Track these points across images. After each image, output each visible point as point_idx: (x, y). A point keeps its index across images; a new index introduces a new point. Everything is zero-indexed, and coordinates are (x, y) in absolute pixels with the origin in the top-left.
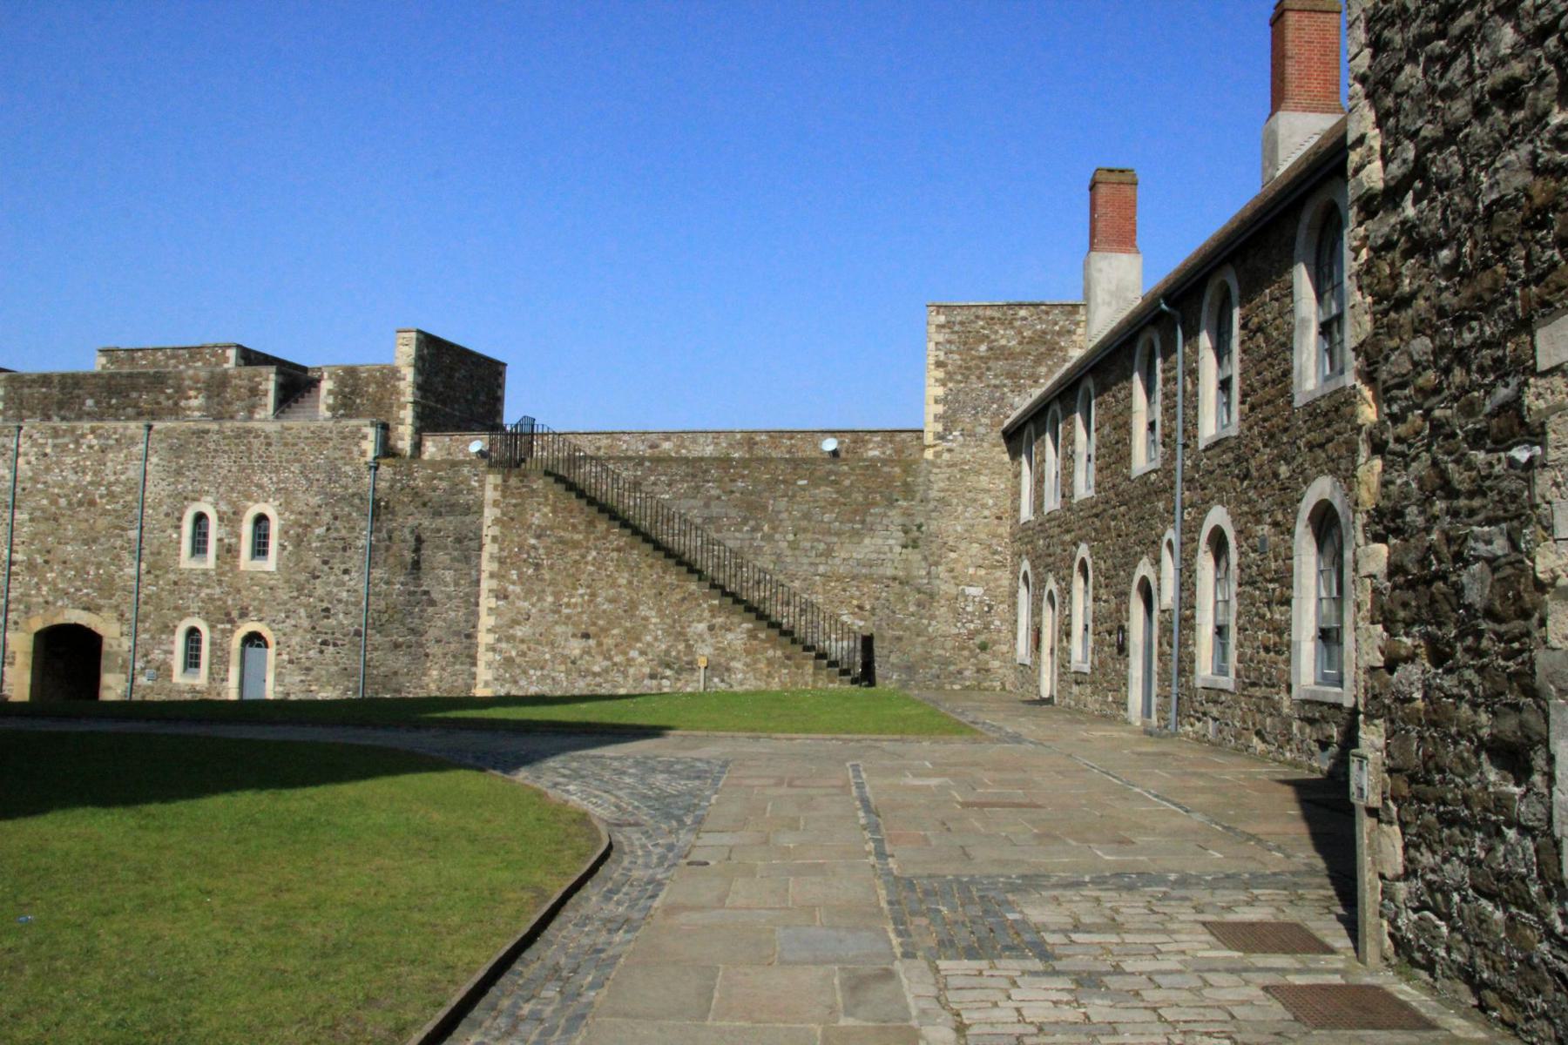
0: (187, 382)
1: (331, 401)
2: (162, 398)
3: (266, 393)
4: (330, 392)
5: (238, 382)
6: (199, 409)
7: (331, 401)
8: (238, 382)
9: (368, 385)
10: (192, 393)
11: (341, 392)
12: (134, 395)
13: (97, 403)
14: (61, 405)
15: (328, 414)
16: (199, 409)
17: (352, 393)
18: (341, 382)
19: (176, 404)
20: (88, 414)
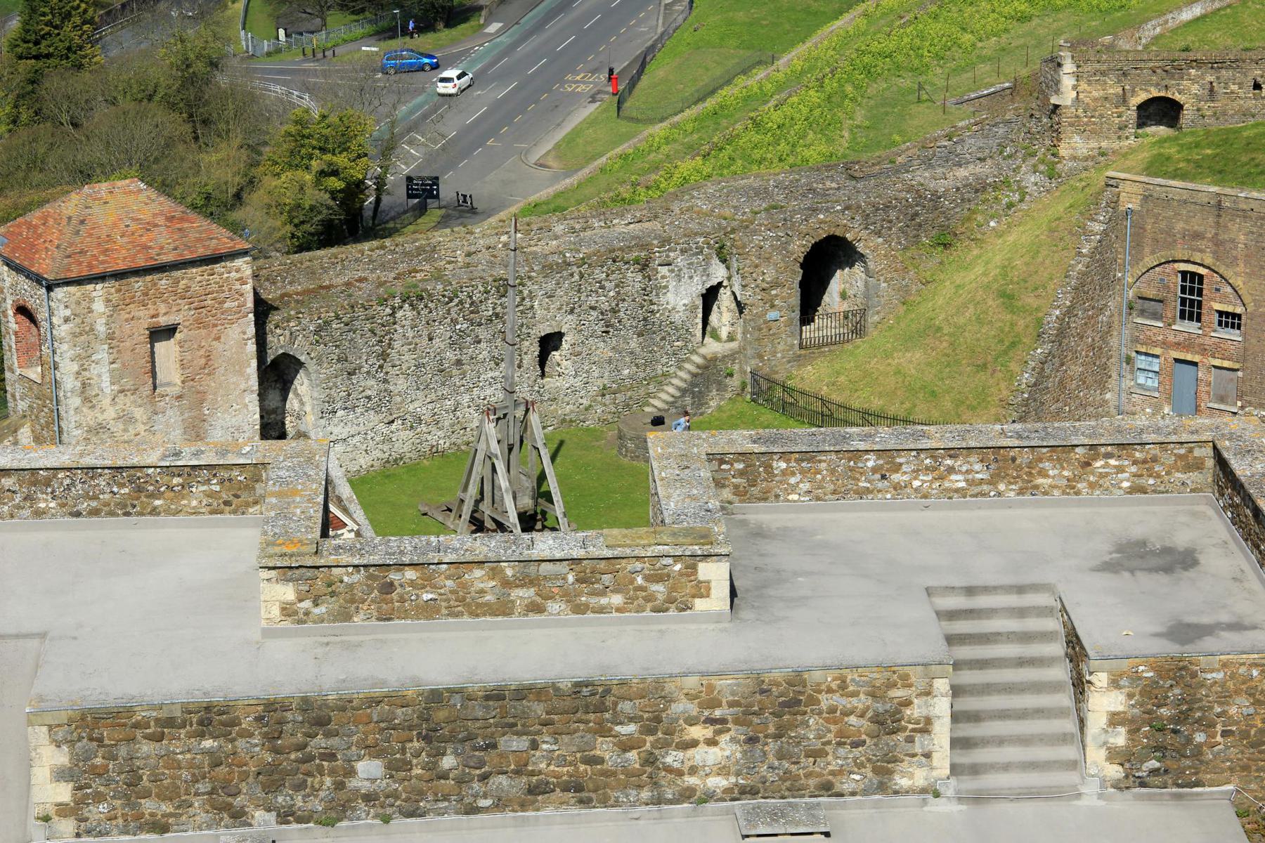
0: (681, 707)
1: (1120, 738)
2: (604, 748)
3: (925, 727)
4: (1115, 720)
5: (837, 700)
6: (723, 770)
7: (1120, 738)
8: (837, 700)
9: (1225, 697)
10: (697, 732)
11: (1150, 718)
12: (519, 744)
13: (396, 767)
14: (272, 779)
15: (1115, 771)
16: (723, 770)
17: (1182, 718)
18: (1150, 694)
19: (650, 760)
20: (369, 798)
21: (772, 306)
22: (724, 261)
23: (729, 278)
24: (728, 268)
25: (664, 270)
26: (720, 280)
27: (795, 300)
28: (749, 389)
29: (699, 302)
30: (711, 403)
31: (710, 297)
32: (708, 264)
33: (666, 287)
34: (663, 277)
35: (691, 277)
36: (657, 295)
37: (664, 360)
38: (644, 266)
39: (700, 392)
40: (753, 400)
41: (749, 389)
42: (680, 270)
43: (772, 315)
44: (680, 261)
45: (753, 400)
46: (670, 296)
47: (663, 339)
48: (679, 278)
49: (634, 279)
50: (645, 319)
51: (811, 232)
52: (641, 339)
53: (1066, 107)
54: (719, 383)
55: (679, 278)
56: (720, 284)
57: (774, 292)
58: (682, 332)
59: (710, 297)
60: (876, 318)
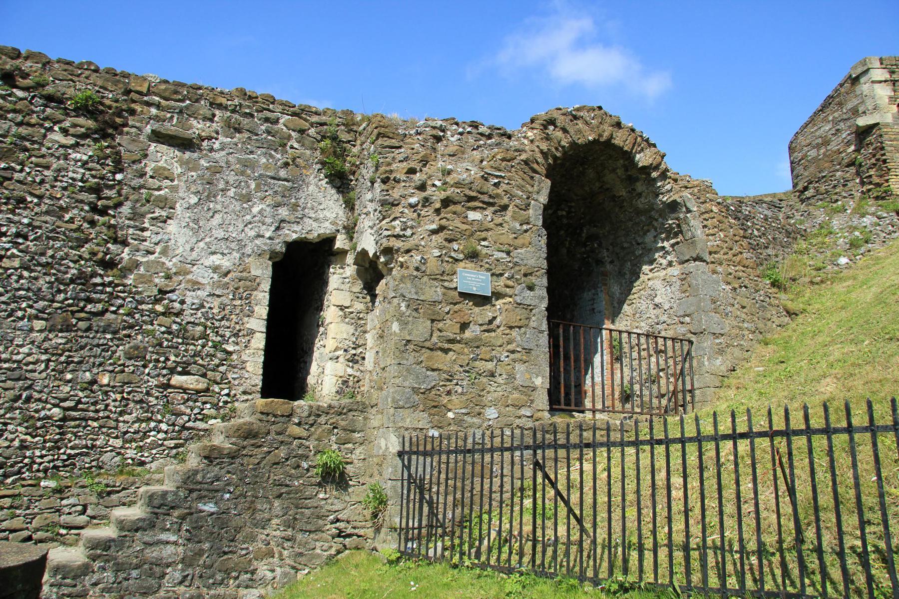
21: (473, 256)
22: (341, 181)
23: (350, 231)
24: (350, 205)
25: (164, 157)
26: (326, 229)
27: (534, 253)
28: (393, 515)
29: (263, 272)
30: (263, 570)
31: (299, 275)
32: (296, 184)
33: (167, 204)
34: (162, 174)
35: (247, 198)
36: (136, 216)
37: (130, 421)
38: (104, 120)
39: (221, 518)
40: (405, 555)
41: (393, 515)
42: (216, 170)
43: (472, 279)
44: (223, 149)
45: (405, 555)
46: (176, 231)
47: (137, 354)
48: (209, 190)
49: (66, 155)
50: (82, 279)
51: (561, 120)
52: (59, 340)
53: (887, 125)
54: (296, 500)
55: (209, 190)
56: (329, 241)
57: (473, 215)
58: (193, 344)
59: (299, 275)
60: (720, 364)
